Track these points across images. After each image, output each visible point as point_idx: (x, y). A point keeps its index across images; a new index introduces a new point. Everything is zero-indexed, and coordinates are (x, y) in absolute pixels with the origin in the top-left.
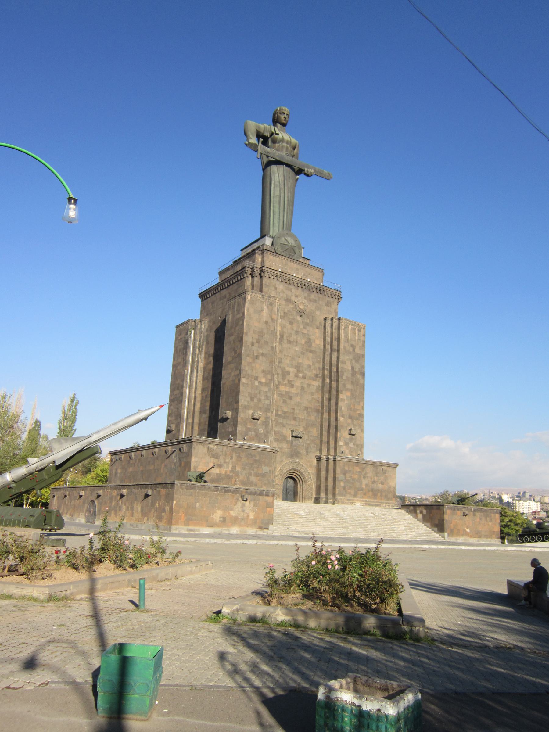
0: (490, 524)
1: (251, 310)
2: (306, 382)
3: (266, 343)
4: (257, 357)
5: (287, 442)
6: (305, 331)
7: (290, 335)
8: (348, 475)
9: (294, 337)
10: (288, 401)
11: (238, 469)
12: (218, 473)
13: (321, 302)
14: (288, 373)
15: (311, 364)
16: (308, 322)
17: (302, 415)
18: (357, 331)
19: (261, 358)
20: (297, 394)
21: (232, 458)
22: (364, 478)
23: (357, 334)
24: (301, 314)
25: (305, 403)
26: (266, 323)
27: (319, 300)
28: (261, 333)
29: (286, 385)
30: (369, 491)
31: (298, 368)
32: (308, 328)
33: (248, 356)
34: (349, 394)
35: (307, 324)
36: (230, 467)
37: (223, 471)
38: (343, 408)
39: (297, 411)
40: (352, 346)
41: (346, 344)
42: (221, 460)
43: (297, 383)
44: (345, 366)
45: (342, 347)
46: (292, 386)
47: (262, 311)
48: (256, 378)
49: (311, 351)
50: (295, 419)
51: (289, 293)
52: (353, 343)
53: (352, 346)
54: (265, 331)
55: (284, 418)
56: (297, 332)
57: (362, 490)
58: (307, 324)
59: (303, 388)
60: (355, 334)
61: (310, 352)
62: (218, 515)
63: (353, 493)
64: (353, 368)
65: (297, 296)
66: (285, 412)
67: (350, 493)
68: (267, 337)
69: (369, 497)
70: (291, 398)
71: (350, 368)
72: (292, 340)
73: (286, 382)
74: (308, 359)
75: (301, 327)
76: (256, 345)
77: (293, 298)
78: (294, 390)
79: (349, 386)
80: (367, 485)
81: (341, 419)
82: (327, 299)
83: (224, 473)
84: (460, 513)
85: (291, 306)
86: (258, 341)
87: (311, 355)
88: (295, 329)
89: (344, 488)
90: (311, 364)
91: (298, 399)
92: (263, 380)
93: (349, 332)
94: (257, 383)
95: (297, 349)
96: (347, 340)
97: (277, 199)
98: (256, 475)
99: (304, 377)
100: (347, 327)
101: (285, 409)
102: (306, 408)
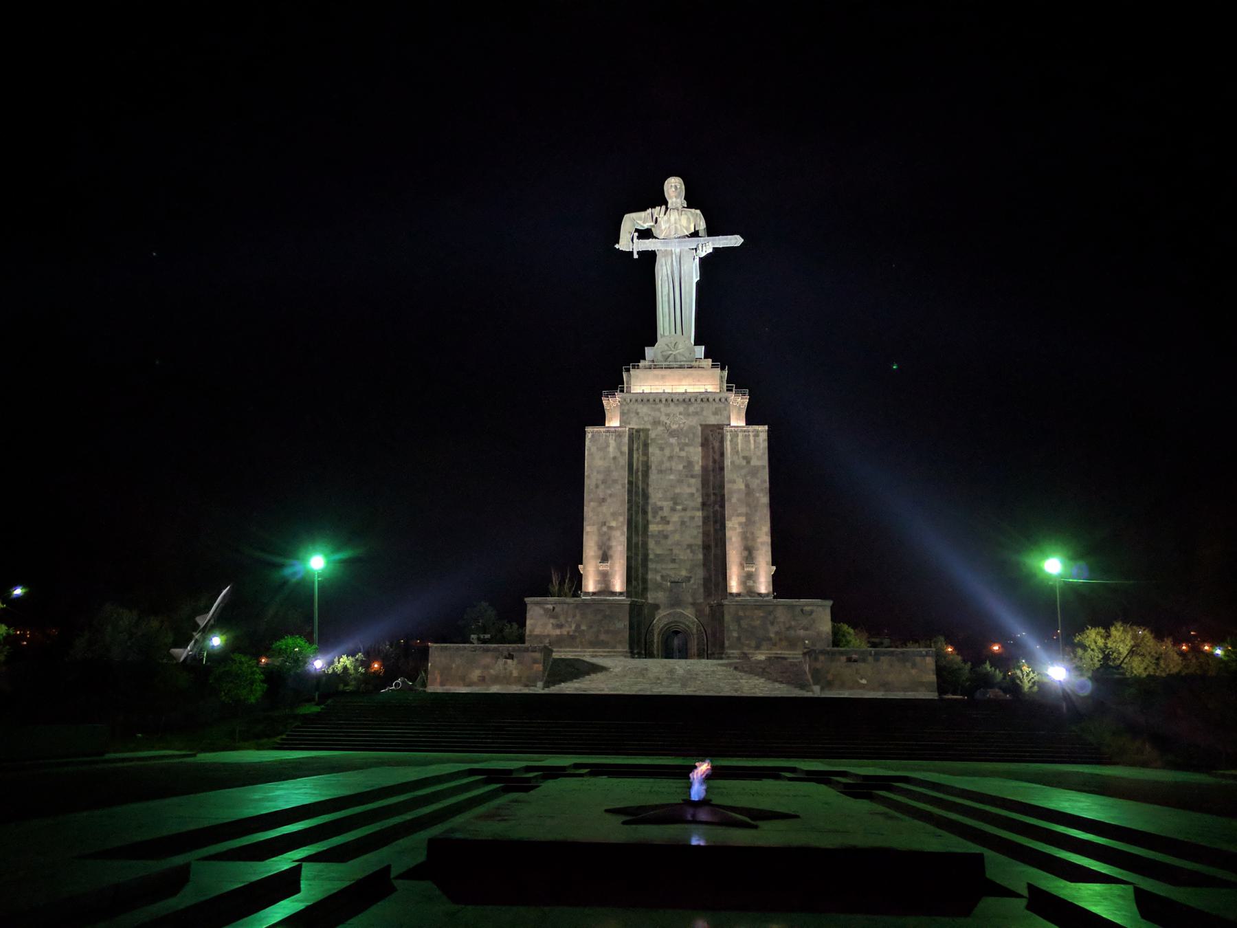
0: (913, 672)
1: (594, 449)
2: (689, 514)
3: (615, 481)
4: (604, 500)
5: (664, 590)
6: (683, 454)
7: (662, 462)
8: (744, 624)
9: (667, 465)
10: (663, 541)
11: (583, 627)
13: (705, 413)
14: (661, 508)
15: (693, 490)
17: (684, 555)
18: (752, 438)
19: (609, 500)
20: (675, 531)
21: (574, 616)
22: (772, 624)
24: (673, 434)
25: (688, 539)
26: (614, 458)
27: (702, 410)
28: (608, 471)
29: (658, 523)
30: (781, 640)
31: (675, 500)
32: (686, 449)
33: (591, 500)
34: (743, 519)
35: (687, 445)
36: (573, 627)
37: (565, 631)
39: (676, 551)
40: (744, 458)
41: (735, 458)
42: (562, 619)
43: (675, 518)
44: (735, 487)
45: (728, 462)
46: (668, 523)
47: (608, 446)
48: (604, 524)
49: (692, 477)
50: (673, 561)
51: (657, 414)
52: (746, 454)
53: (744, 458)
54: (613, 467)
55: (657, 562)
56: (671, 458)
57: (770, 639)
58: (687, 445)
59: (683, 523)
62: (476, 674)
63: (753, 644)
64: (747, 486)
65: (668, 415)
66: (657, 556)
67: (748, 646)
68: (615, 475)
69: (781, 649)
70: (666, 537)
71: (743, 487)
72: (664, 467)
73: (658, 519)
74: (689, 486)
75: (677, 449)
76: (602, 487)
77: (663, 418)
78: (670, 528)
79: (743, 510)
80: (777, 633)
82: (715, 406)
84: (844, 658)
85: (660, 428)
86: (604, 482)
87: (693, 481)
88: (667, 452)
89: (739, 639)
90: (693, 490)
91: (677, 537)
94: (605, 529)
95: (672, 477)
96: (735, 451)
97: (665, 299)
98: (607, 632)
99: (684, 510)
101: (659, 552)
102: (690, 546)
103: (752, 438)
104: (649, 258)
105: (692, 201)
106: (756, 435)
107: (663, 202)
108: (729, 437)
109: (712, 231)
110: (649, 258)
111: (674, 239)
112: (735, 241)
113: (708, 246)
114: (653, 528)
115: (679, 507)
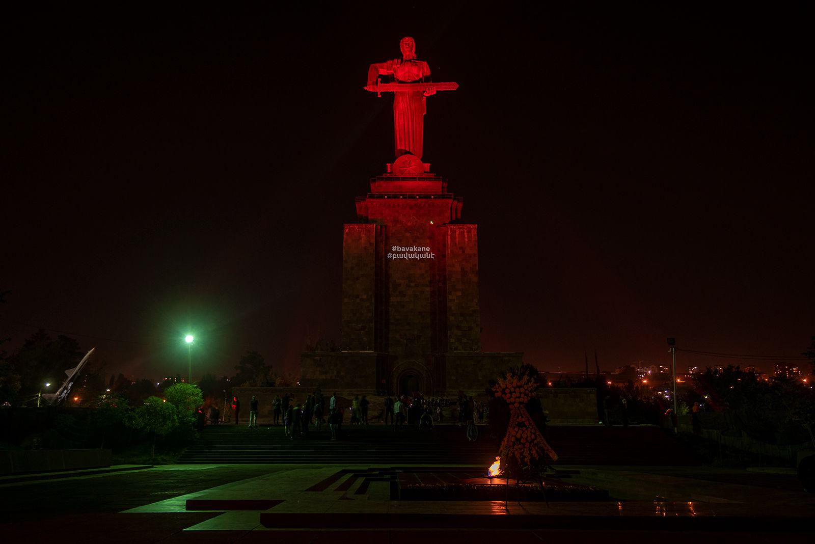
12: (325, 378)
16: (418, 235)
18: (466, 233)
23: (466, 236)
38: (453, 308)
45: (448, 251)
47: (361, 239)
60: (464, 236)
61: (422, 262)
81: (452, 318)
83: (329, 378)
92: (365, 297)
93: (457, 236)
94: (358, 300)
100: (454, 232)
103: (466, 233)
104: (389, 98)
105: (422, 54)
106: (469, 231)
107: (399, 55)
108: (449, 233)
109: (434, 78)
110: (389, 98)
111: (405, 82)
112: (452, 86)
113: (431, 90)
114: (393, 300)
115: (413, 284)
